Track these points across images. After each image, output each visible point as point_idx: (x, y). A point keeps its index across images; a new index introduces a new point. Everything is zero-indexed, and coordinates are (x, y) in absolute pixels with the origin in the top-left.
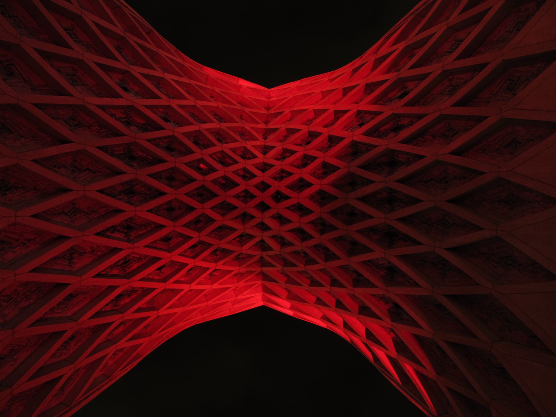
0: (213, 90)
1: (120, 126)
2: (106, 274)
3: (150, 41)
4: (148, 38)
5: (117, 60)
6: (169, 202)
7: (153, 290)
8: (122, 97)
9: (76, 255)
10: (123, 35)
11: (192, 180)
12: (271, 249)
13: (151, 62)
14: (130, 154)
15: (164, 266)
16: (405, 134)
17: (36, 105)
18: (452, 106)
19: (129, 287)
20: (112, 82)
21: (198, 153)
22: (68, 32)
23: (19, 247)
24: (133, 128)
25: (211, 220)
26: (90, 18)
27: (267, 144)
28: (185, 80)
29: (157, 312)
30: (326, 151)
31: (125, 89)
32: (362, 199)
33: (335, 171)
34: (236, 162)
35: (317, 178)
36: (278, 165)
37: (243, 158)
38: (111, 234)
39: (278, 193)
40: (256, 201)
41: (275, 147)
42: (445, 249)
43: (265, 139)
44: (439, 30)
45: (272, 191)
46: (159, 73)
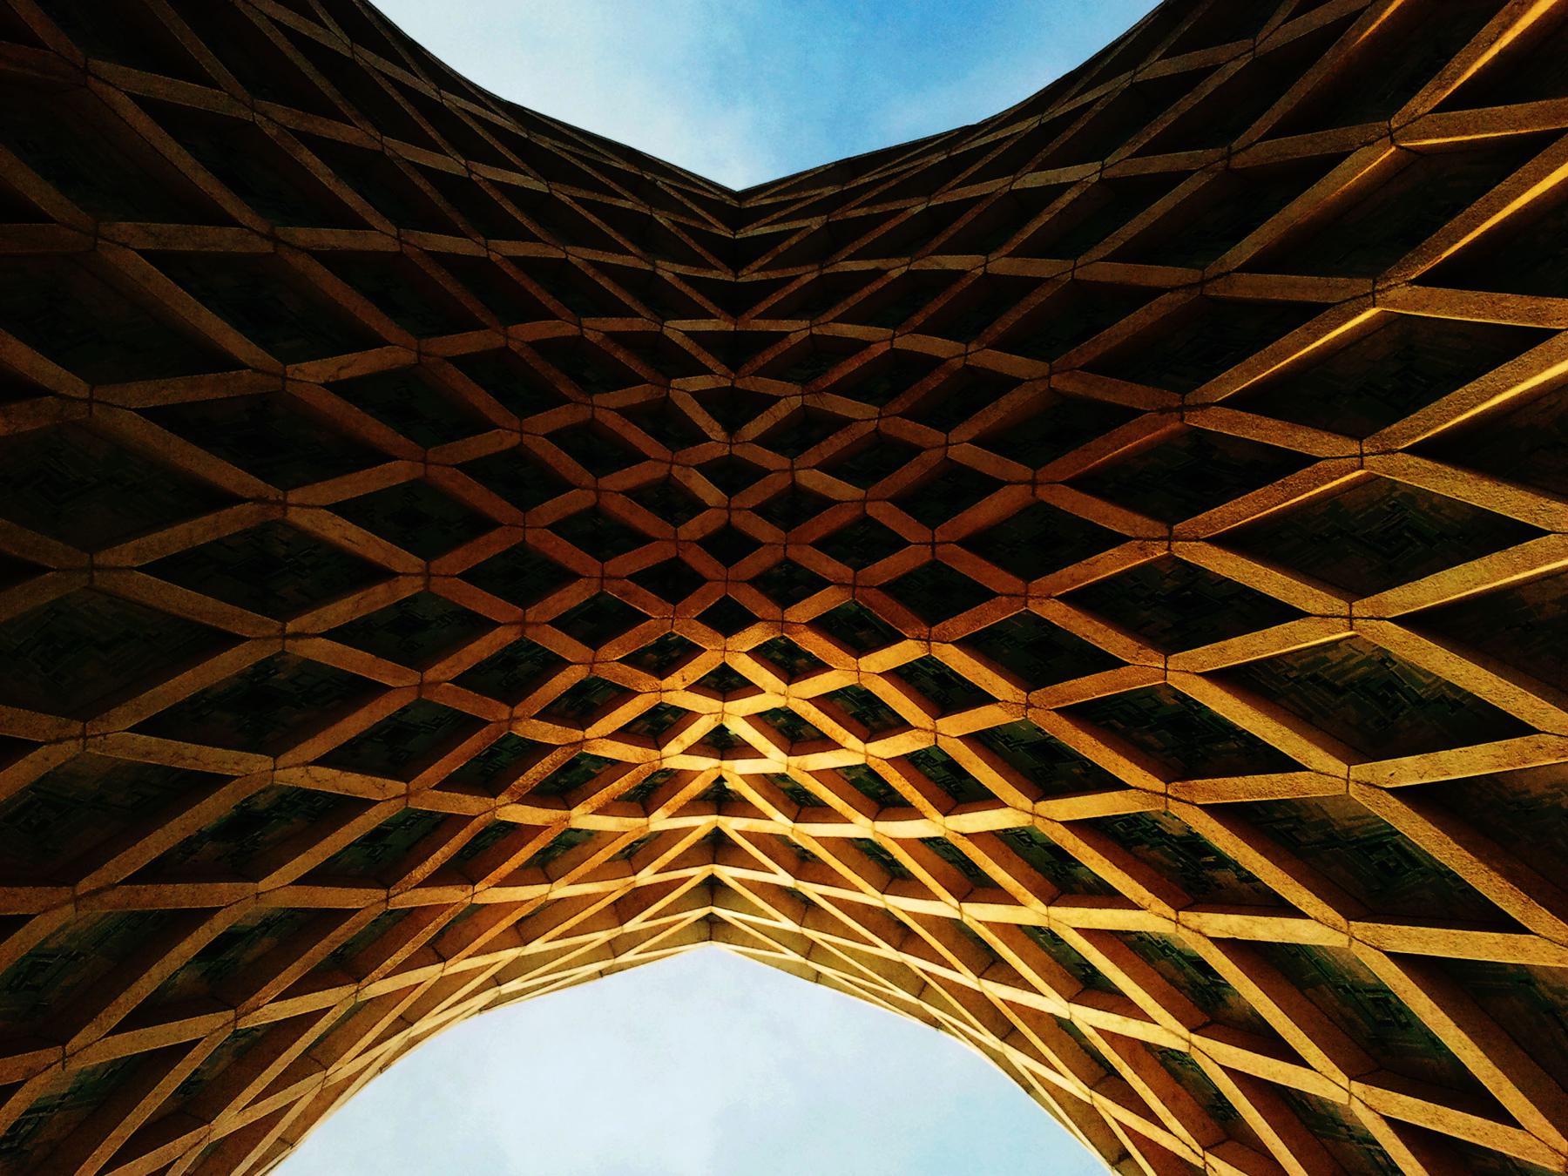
5: (1231, 1072)
7: (1114, 257)
8: (1217, 941)
16: (212, 809)
18: (25, 919)
19: (1202, 268)
25: (906, 502)
27: (714, 762)
28: (996, 991)
40: (752, 564)
45: (699, 602)
46: (1087, 1018)
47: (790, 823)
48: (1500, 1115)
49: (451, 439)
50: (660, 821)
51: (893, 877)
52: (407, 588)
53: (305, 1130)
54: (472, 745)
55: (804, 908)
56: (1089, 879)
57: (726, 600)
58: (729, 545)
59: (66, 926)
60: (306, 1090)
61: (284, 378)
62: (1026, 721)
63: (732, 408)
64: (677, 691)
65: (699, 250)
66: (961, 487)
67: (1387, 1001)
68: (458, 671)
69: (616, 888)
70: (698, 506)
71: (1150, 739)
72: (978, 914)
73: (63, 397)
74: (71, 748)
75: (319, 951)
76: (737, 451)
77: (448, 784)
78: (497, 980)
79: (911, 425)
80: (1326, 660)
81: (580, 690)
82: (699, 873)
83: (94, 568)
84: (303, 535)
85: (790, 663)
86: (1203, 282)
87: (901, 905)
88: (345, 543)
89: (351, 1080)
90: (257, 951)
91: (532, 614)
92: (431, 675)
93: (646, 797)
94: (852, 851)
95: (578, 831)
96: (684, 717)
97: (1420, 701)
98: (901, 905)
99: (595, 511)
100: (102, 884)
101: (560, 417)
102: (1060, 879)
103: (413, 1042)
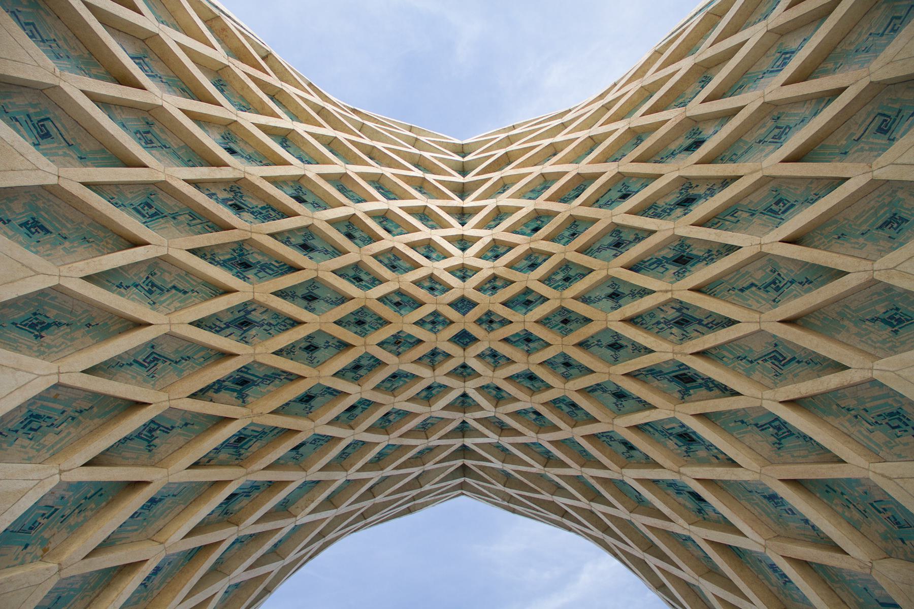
0: (374, 147)
1: (226, 214)
2: (209, 461)
6: (309, 337)
7: (287, 483)
10: (226, 63)
11: (344, 299)
12: (479, 408)
14: (241, 260)
15: (302, 445)
17: (87, 185)
20: (211, 142)
21: (354, 254)
23: (65, 424)
24: (245, 215)
25: (378, 364)
26: (171, 37)
27: (466, 233)
28: (328, 131)
29: (294, 519)
31: (232, 152)
32: (632, 321)
33: (584, 276)
34: (417, 266)
35: (555, 288)
38: (215, 395)
40: (453, 330)
41: (481, 238)
44: (753, 35)
46: (285, 122)
47: (429, 205)
49: (598, 385)
51: (378, 182)
53: (650, 58)
54: (581, 240)
55: (419, 163)
56: (285, 188)
58: (464, 339)
59: (765, 156)
60: (650, 78)
61: (674, 410)
62: (318, 262)
63: (464, 403)
64: (487, 268)
65: (481, 473)
66: (355, 371)
67: (146, 143)
68: (590, 275)
69: (508, 171)
70: (480, 356)
71: (260, 258)
72: (338, 167)
76: (462, 384)
77: (594, 221)
78: (564, 126)
79: (378, 401)
80: (180, 302)
81: (533, 266)
82: (470, 178)
84: (665, 339)
85: (433, 284)
86: (247, 474)
87: (375, 169)
88: (645, 335)
89: (630, 81)
92: (603, 273)
93: (499, 214)
94: (397, 193)
95: (530, 198)
96: (481, 255)
97: (136, 286)
98: (375, 169)
99: (529, 353)
101: (548, 396)
102: (300, 189)
103: (602, 96)
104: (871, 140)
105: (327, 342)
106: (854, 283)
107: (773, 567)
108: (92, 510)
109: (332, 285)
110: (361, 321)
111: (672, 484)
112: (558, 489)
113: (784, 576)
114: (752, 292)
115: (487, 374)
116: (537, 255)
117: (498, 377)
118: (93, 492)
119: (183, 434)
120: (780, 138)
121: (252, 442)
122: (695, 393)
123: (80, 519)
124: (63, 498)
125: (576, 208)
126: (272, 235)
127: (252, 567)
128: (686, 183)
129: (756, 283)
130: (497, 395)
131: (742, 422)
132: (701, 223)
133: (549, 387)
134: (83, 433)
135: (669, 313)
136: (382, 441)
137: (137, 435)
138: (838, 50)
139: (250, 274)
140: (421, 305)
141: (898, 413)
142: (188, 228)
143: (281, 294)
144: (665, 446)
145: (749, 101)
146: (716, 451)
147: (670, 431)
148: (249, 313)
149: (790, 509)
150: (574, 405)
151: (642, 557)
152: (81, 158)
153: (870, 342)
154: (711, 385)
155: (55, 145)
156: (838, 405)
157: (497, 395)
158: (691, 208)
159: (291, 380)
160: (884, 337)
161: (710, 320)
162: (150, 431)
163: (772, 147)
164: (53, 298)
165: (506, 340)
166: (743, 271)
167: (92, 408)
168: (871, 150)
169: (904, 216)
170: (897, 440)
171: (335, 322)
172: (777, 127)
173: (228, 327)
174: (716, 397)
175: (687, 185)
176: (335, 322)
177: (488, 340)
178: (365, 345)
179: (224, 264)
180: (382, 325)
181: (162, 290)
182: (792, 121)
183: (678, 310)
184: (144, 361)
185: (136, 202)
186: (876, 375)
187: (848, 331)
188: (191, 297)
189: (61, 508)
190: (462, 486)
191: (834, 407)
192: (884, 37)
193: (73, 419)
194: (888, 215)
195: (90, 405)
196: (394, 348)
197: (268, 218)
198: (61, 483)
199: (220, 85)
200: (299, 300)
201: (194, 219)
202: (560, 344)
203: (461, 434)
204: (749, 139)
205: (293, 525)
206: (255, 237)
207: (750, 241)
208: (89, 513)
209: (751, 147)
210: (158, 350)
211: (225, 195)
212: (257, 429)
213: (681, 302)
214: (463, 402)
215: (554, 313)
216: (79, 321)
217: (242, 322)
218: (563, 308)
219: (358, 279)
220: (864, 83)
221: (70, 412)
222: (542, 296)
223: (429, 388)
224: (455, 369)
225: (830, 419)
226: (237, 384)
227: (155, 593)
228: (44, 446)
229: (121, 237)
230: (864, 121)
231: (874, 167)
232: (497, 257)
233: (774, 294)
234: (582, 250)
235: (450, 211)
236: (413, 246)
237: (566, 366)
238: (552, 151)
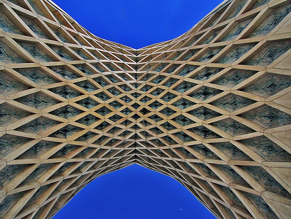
1: (59, 77)
3: (73, 28)
4: (72, 26)
9: (38, 147)
10: (60, 26)
11: (98, 104)
13: (75, 40)
14: (64, 91)
21: (101, 89)
22: (30, 27)
23: (8, 146)
24: (66, 77)
29: (81, 173)
30: (169, 86)
31: (61, 56)
32: (189, 112)
34: (121, 93)
36: (144, 94)
37: (125, 90)
39: (144, 109)
40: (133, 114)
42: (235, 141)
43: (136, 79)
44: (230, 22)
45: (140, 108)
46: (79, 46)
48: (16, 40)
50: (145, 72)
52: (185, 110)
54: (174, 86)
55: (122, 58)
57: (136, 109)
58: (136, 117)
63: (136, 137)
67: (34, 54)
69: (151, 61)
70: (141, 122)
72: (96, 61)
73: (233, 140)
74: (233, 89)
75: (196, 55)
76: (135, 131)
80: (45, 106)
81: (158, 94)
83: (229, 115)
85: (126, 99)
90: (205, 55)
91: (166, 106)
95: (158, 71)
97: (31, 101)
98: (108, 60)
100: (228, 68)
104: (266, 59)
105: (92, 118)
106: (259, 105)
107: (231, 191)
108: (17, 173)
109: (94, 99)
110: (103, 111)
111: (200, 164)
112: (165, 164)
113: (234, 194)
114: (227, 105)
115: (143, 127)
116: (160, 90)
117: (147, 129)
118: (17, 167)
119: (46, 148)
120: (238, 56)
121: (68, 150)
122: (209, 136)
123: (13, 176)
124: (7, 170)
125: (172, 75)
126: (74, 83)
127: (68, 189)
128: (208, 69)
129: (229, 102)
130: (146, 134)
131: (223, 146)
132: (212, 82)
133: (163, 132)
134: (14, 149)
135: (201, 110)
136: (109, 148)
137: (32, 149)
138: (257, 29)
139: (67, 96)
140: (122, 106)
141: (271, 146)
142: (47, 81)
143: (77, 102)
144: (199, 152)
145: (228, 43)
146: (214, 154)
147: (201, 148)
148: (67, 108)
149: (237, 174)
150: (170, 138)
151: (191, 186)
152: (12, 60)
153: (263, 123)
154: (214, 134)
155: (4, 56)
156: (253, 143)
157: (146, 134)
158: (209, 77)
159: (81, 130)
160: (268, 122)
161: (214, 113)
162: (35, 147)
163: (235, 59)
164: (4, 106)
165: (149, 117)
166: (225, 98)
167: (17, 140)
168: (266, 62)
169: (275, 84)
170: (271, 155)
171: (95, 111)
172: (237, 52)
173: (60, 113)
174: (215, 138)
175: (208, 69)
176: (95, 111)
177: (143, 117)
178: (104, 118)
179: (60, 93)
180: (110, 112)
181: (39, 102)
182: (242, 51)
183: (204, 110)
184: (34, 125)
185: (31, 74)
186: (265, 134)
187: (257, 119)
188: (48, 104)
189: (7, 173)
190: (135, 161)
191: (252, 143)
192: (272, 26)
193: (11, 144)
194: (271, 83)
195: (16, 140)
196: (114, 119)
197: (73, 78)
198: (7, 165)
199: (57, 34)
200: (83, 104)
201: (49, 79)
202: (166, 119)
203: (135, 146)
204: (228, 56)
205: (81, 175)
206: (69, 84)
207: (227, 89)
208: (16, 174)
209: (228, 58)
210: (38, 121)
211: (60, 71)
212: (70, 145)
213: (205, 107)
214: (135, 136)
215: (164, 109)
216: (12, 113)
217: (65, 111)
218: (168, 107)
219: (103, 97)
220: (265, 41)
221: (10, 142)
222: (161, 103)
223: (125, 132)
224: (133, 126)
225: (250, 147)
226: (63, 131)
227: (37, 198)
228: (1, 154)
229: (26, 85)
230: (264, 53)
231: (267, 69)
232: (147, 90)
233: (234, 106)
234: (174, 89)
235: (132, 74)
236: (120, 86)
237: (168, 126)
238: (165, 55)
